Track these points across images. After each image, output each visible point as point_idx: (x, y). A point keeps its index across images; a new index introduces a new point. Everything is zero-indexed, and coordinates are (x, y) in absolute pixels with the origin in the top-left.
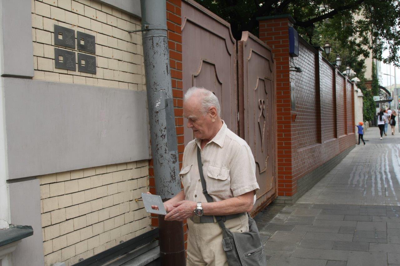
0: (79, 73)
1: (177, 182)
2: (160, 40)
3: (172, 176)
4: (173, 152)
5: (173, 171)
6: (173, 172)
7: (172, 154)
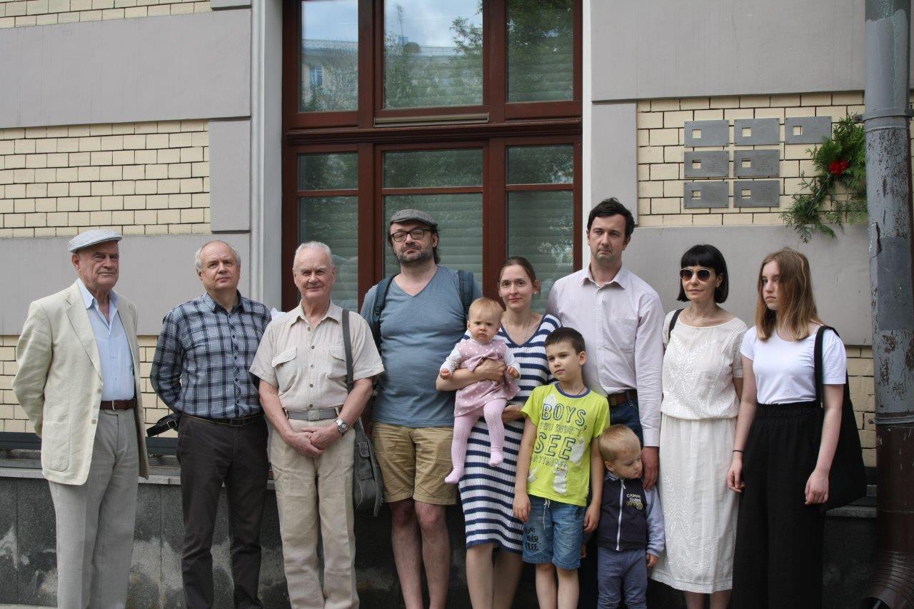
0: (737, 210)
1: (892, 386)
2: (874, 138)
3: (882, 374)
4: (888, 333)
5: (883, 365)
6: (885, 367)
7: (884, 336)
